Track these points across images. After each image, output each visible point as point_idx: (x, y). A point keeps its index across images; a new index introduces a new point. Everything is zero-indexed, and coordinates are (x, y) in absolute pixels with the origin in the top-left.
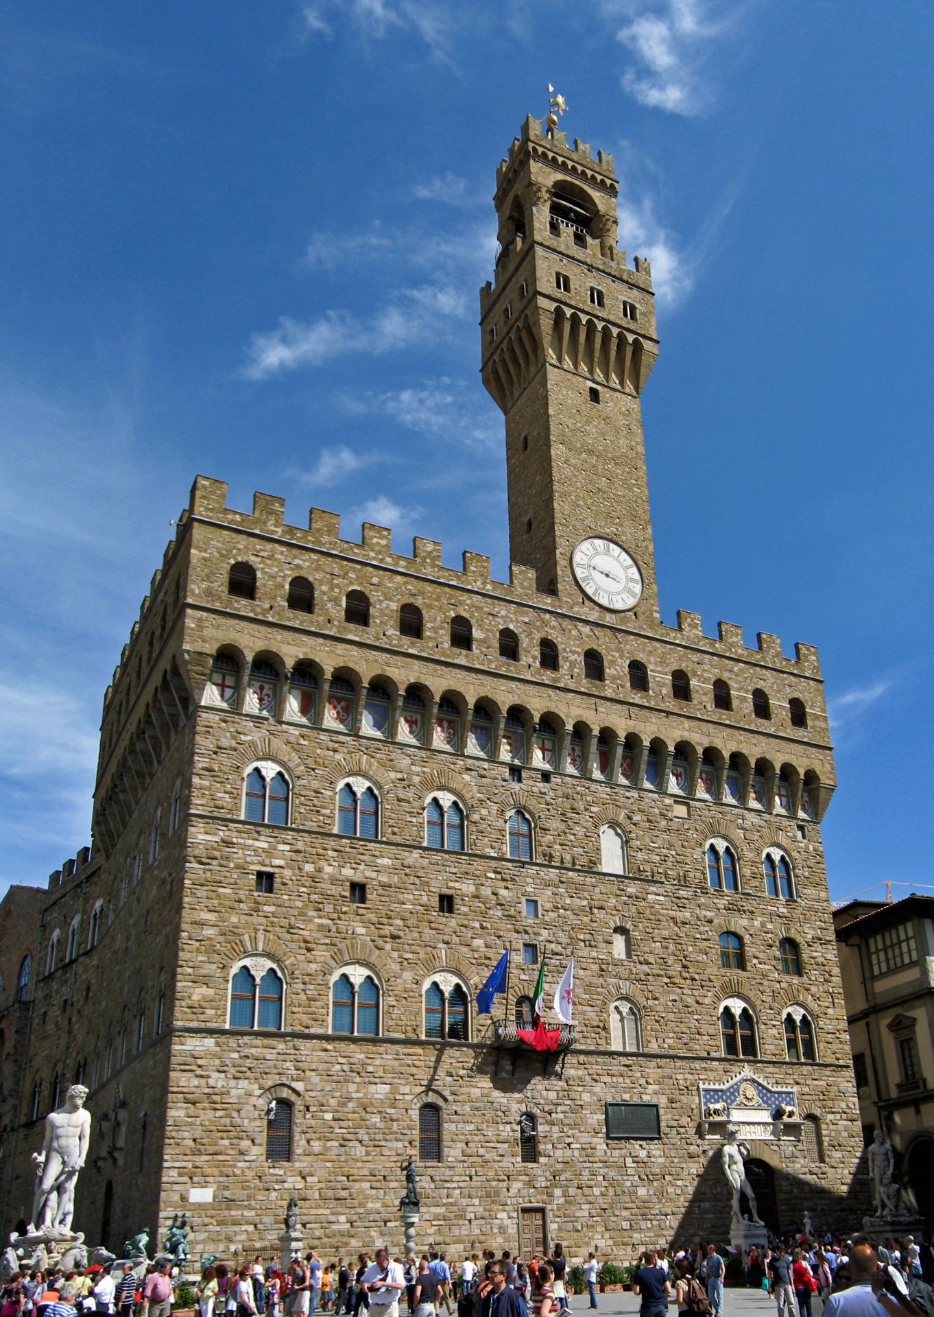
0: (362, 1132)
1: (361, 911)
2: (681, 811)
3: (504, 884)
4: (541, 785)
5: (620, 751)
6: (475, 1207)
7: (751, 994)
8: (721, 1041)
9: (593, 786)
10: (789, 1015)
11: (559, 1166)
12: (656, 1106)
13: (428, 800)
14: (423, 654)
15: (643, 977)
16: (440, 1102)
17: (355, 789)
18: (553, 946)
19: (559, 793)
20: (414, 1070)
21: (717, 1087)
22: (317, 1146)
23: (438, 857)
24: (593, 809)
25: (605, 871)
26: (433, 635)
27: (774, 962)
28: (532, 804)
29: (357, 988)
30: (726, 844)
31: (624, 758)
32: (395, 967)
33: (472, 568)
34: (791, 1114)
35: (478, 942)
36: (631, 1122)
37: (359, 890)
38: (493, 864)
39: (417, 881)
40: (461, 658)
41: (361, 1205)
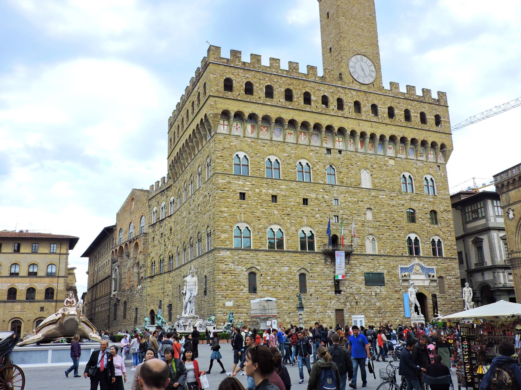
0: (280, 283)
1: (276, 205)
2: (392, 162)
3: (326, 193)
4: (339, 155)
5: (368, 140)
6: (320, 309)
7: (418, 232)
8: (407, 250)
9: (358, 154)
10: (433, 239)
11: (349, 295)
12: (383, 273)
13: (298, 163)
14: (295, 108)
15: (377, 227)
16: (306, 273)
17: (271, 160)
18: (344, 216)
19: (345, 158)
20: (297, 262)
21: (405, 266)
22: (265, 288)
23: (302, 184)
24: (358, 163)
25: (363, 186)
26: (297, 100)
27: (427, 220)
28: (335, 163)
29: (275, 233)
30: (409, 174)
31: (370, 143)
32: (289, 225)
33: (311, 72)
34: (433, 276)
35: (318, 216)
36: (374, 279)
37: (274, 198)
38: (322, 186)
39: (295, 194)
40: (308, 108)
41: (282, 308)
